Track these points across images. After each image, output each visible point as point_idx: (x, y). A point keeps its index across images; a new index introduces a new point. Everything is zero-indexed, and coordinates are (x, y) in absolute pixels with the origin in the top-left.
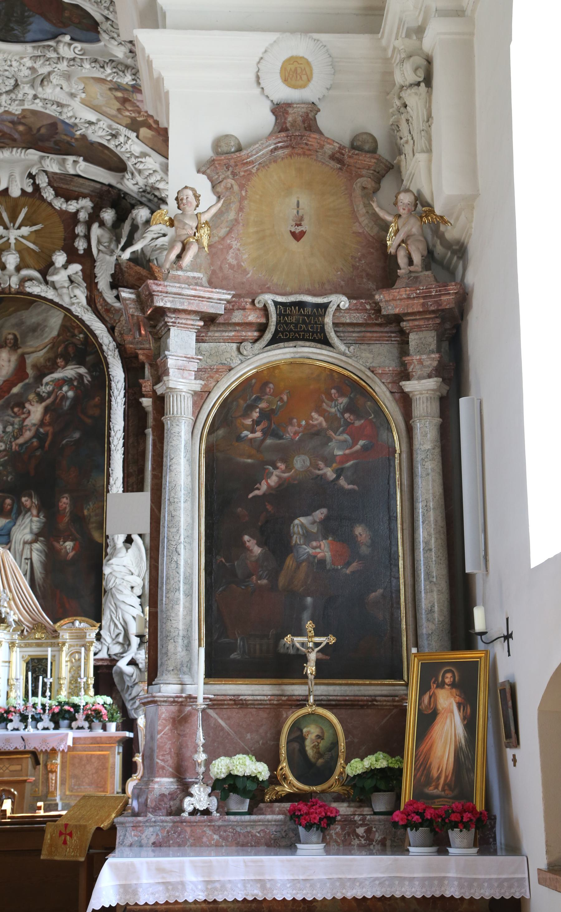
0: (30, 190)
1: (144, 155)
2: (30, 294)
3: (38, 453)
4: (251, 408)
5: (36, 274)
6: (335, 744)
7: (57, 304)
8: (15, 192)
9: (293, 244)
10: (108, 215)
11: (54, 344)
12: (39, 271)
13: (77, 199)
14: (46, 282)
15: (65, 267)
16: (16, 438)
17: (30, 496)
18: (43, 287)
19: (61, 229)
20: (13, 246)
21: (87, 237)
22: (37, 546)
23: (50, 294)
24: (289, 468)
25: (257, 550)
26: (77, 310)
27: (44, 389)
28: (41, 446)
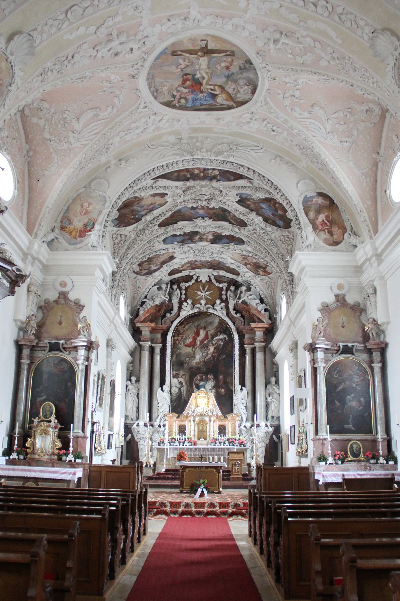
0: (208, 280)
1: (247, 272)
2: (209, 312)
3: (213, 362)
4: (335, 370)
5: (211, 306)
6: (360, 449)
7: (217, 315)
8: (204, 281)
9: (342, 329)
10: (233, 288)
11: (217, 328)
12: (212, 305)
13: (222, 283)
14: (214, 309)
15: (220, 304)
16: (206, 357)
18: (213, 310)
19: (218, 292)
21: (226, 295)
22: (213, 390)
23: (215, 313)
24: (345, 384)
25: (338, 404)
26: (224, 318)
27: (214, 342)
28: (214, 360)
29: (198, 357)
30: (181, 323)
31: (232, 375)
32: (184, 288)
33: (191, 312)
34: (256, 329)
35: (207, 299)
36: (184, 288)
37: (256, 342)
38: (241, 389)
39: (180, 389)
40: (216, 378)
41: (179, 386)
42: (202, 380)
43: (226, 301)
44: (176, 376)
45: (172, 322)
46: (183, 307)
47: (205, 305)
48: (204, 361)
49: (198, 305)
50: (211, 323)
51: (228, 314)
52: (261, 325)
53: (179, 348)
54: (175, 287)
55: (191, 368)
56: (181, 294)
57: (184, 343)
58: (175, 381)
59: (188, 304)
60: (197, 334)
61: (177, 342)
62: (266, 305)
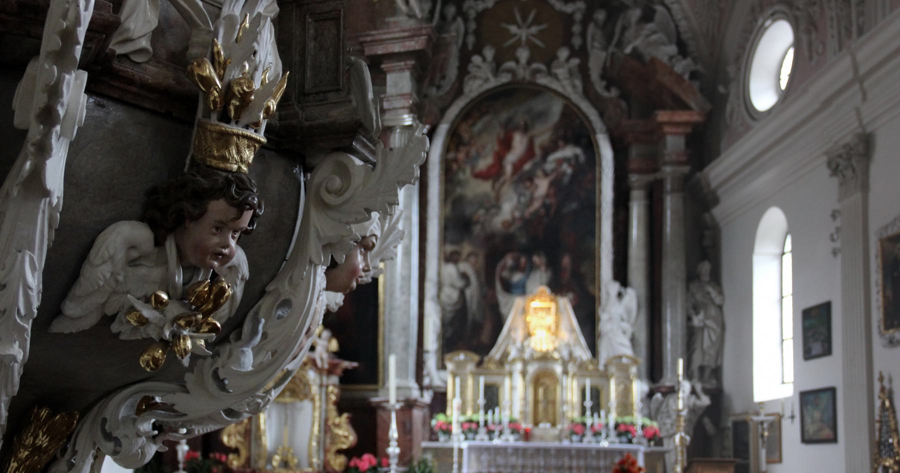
2: (538, 85)
5: (543, 67)
11: (557, 128)
17: (539, 256)
20: (523, 43)
21: (583, 35)
23: (555, 85)
27: (549, 166)
29: (508, 208)
30: (466, 115)
31: (591, 256)
32: (472, 14)
33: (493, 83)
34: (667, 129)
35: (532, 47)
36: (472, 14)
37: (665, 164)
38: (620, 295)
39: (462, 293)
40: (553, 265)
41: (460, 283)
42: (516, 268)
43: (582, 53)
44: (450, 258)
45: (443, 111)
46: (471, 68)
47: (529, 62)
48: (522, 218)
49: (511, 64)
50: (541, 116)
51: (588, 92)
52: (683, 116)
53: (460, 183)
54: (451, 10)
55: (490, 237)
56: (466, 33)
57: (473, 168)
58: (450, 270)
59: (484, 59)
60: (506, 145)
61: (455, 166)
62: (695, 60)
